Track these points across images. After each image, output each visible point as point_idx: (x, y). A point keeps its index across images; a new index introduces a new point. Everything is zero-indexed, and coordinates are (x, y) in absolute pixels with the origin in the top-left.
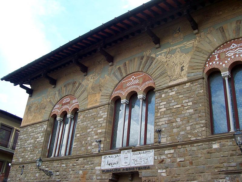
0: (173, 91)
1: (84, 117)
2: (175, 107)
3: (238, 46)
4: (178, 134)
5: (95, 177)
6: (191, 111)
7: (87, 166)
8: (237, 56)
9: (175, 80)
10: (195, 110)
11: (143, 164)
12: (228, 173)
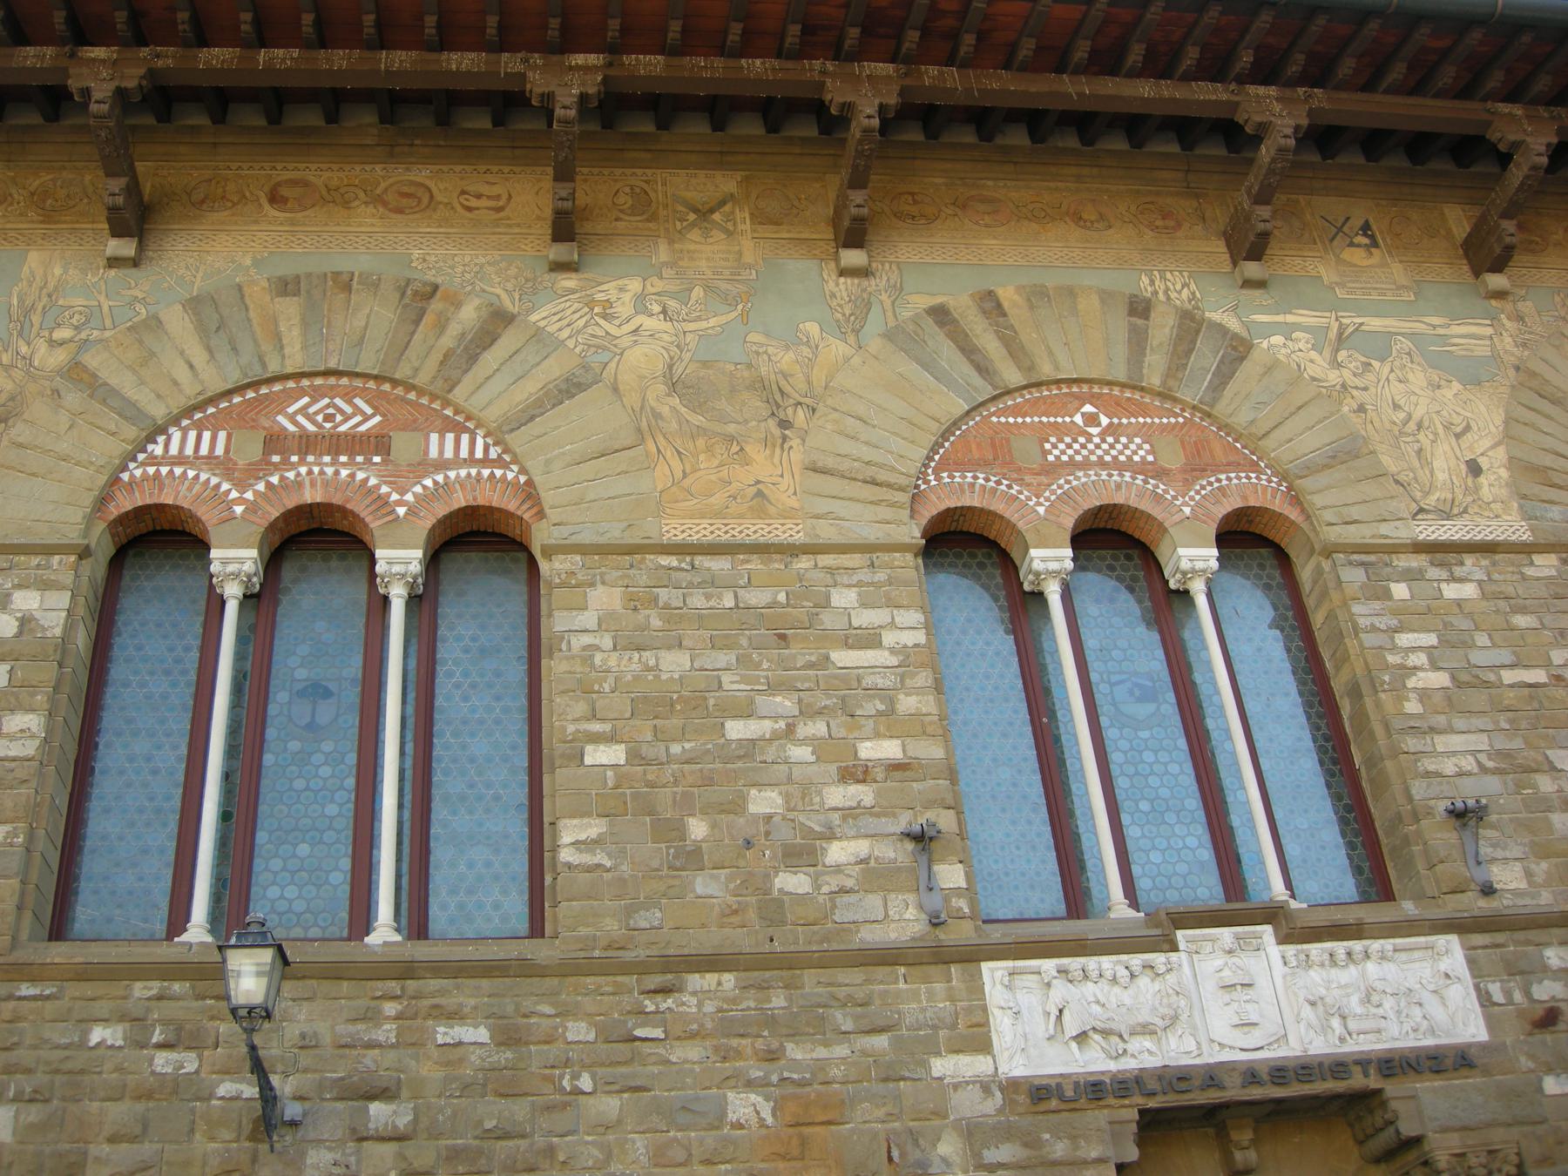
1: (634, 603)
2: (1508, 677)
7: (821, 1052)
11: (1397, 1033)
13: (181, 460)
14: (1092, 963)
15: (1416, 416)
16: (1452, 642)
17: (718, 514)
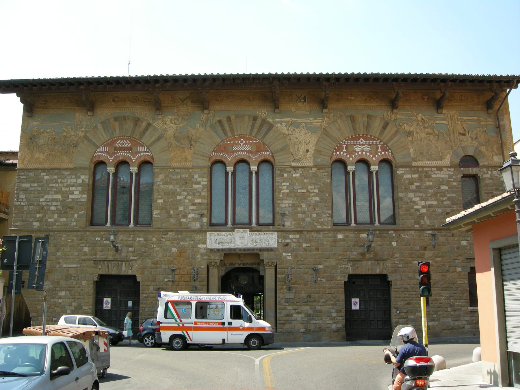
2: (299, 191)
4: (303, 220)
5: (199, 256)
6: (317, 199)
7: (184, 243)
9: (298, 160)
11: (264, 246)
12: (350, 260)
13: (102, 152)
14: (222, 233)
16: (292, 184)
17: (180, 162)
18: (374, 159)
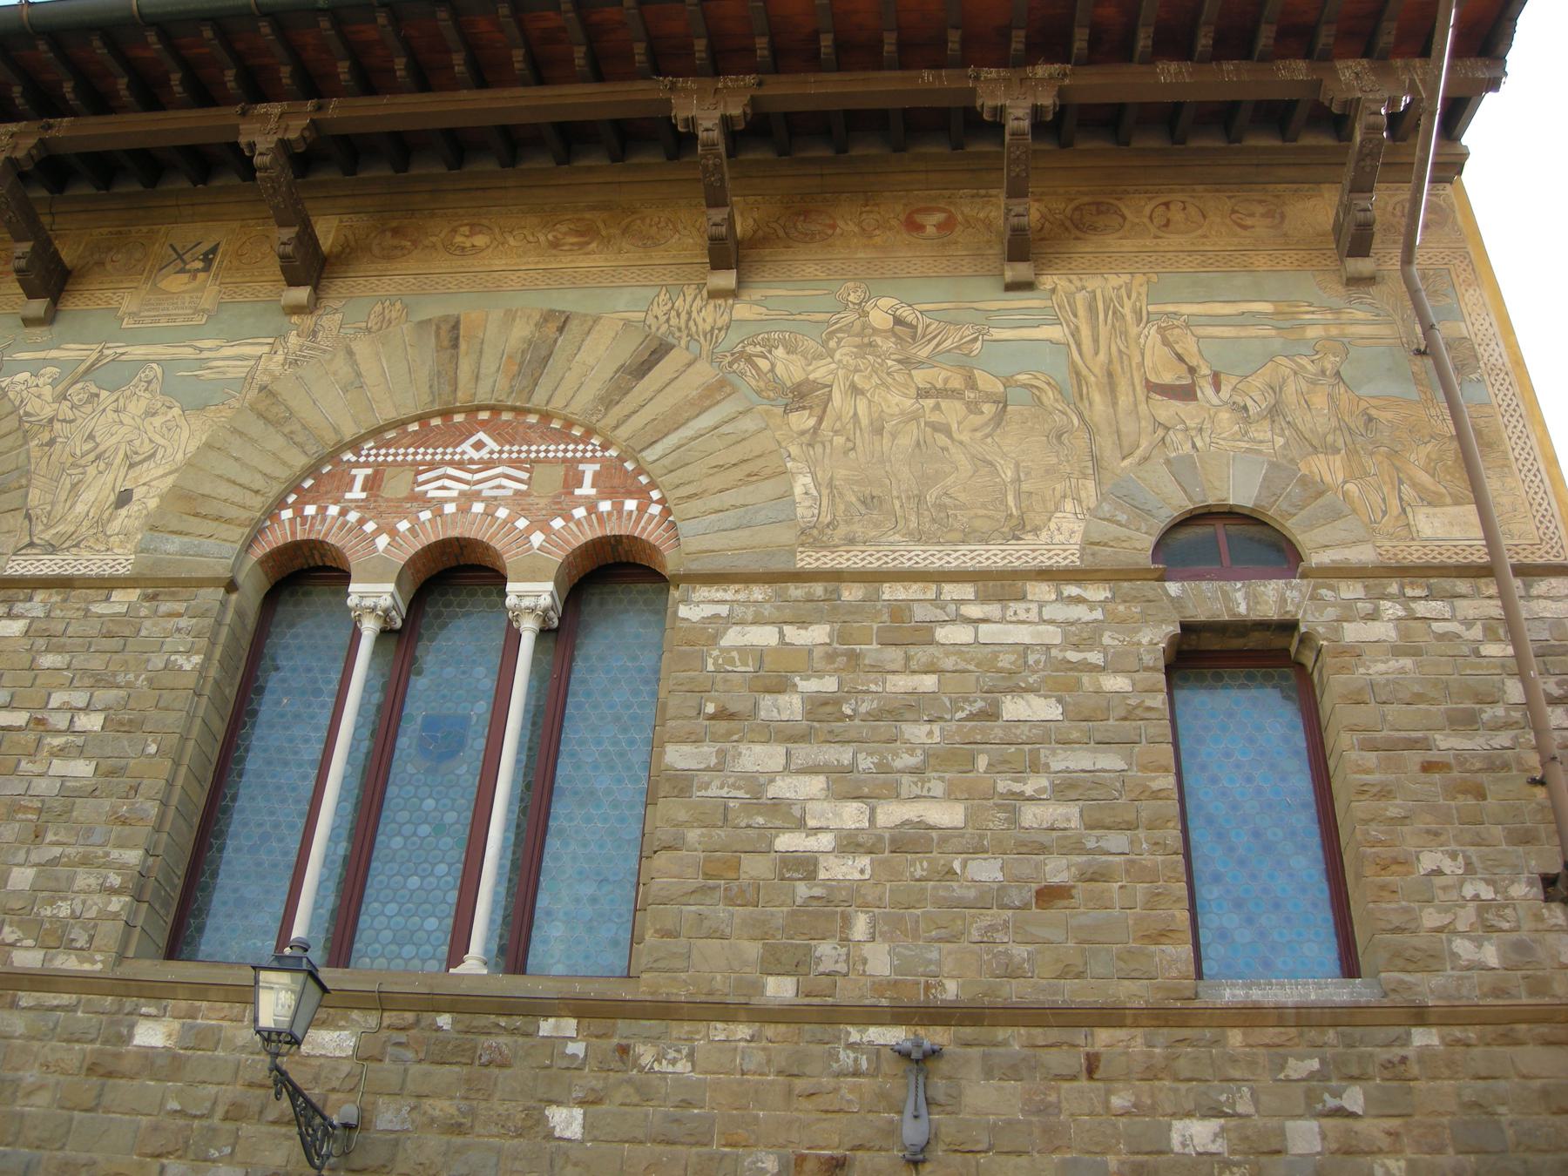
0: (15, 611)
3: (505, 456)
6: (82, 769)
8: (478, 507)
9: (52, 548)
10: (103, 768)
15: (101, 448)
18: (537, 539)
